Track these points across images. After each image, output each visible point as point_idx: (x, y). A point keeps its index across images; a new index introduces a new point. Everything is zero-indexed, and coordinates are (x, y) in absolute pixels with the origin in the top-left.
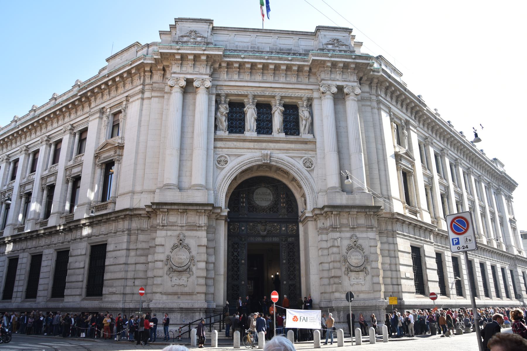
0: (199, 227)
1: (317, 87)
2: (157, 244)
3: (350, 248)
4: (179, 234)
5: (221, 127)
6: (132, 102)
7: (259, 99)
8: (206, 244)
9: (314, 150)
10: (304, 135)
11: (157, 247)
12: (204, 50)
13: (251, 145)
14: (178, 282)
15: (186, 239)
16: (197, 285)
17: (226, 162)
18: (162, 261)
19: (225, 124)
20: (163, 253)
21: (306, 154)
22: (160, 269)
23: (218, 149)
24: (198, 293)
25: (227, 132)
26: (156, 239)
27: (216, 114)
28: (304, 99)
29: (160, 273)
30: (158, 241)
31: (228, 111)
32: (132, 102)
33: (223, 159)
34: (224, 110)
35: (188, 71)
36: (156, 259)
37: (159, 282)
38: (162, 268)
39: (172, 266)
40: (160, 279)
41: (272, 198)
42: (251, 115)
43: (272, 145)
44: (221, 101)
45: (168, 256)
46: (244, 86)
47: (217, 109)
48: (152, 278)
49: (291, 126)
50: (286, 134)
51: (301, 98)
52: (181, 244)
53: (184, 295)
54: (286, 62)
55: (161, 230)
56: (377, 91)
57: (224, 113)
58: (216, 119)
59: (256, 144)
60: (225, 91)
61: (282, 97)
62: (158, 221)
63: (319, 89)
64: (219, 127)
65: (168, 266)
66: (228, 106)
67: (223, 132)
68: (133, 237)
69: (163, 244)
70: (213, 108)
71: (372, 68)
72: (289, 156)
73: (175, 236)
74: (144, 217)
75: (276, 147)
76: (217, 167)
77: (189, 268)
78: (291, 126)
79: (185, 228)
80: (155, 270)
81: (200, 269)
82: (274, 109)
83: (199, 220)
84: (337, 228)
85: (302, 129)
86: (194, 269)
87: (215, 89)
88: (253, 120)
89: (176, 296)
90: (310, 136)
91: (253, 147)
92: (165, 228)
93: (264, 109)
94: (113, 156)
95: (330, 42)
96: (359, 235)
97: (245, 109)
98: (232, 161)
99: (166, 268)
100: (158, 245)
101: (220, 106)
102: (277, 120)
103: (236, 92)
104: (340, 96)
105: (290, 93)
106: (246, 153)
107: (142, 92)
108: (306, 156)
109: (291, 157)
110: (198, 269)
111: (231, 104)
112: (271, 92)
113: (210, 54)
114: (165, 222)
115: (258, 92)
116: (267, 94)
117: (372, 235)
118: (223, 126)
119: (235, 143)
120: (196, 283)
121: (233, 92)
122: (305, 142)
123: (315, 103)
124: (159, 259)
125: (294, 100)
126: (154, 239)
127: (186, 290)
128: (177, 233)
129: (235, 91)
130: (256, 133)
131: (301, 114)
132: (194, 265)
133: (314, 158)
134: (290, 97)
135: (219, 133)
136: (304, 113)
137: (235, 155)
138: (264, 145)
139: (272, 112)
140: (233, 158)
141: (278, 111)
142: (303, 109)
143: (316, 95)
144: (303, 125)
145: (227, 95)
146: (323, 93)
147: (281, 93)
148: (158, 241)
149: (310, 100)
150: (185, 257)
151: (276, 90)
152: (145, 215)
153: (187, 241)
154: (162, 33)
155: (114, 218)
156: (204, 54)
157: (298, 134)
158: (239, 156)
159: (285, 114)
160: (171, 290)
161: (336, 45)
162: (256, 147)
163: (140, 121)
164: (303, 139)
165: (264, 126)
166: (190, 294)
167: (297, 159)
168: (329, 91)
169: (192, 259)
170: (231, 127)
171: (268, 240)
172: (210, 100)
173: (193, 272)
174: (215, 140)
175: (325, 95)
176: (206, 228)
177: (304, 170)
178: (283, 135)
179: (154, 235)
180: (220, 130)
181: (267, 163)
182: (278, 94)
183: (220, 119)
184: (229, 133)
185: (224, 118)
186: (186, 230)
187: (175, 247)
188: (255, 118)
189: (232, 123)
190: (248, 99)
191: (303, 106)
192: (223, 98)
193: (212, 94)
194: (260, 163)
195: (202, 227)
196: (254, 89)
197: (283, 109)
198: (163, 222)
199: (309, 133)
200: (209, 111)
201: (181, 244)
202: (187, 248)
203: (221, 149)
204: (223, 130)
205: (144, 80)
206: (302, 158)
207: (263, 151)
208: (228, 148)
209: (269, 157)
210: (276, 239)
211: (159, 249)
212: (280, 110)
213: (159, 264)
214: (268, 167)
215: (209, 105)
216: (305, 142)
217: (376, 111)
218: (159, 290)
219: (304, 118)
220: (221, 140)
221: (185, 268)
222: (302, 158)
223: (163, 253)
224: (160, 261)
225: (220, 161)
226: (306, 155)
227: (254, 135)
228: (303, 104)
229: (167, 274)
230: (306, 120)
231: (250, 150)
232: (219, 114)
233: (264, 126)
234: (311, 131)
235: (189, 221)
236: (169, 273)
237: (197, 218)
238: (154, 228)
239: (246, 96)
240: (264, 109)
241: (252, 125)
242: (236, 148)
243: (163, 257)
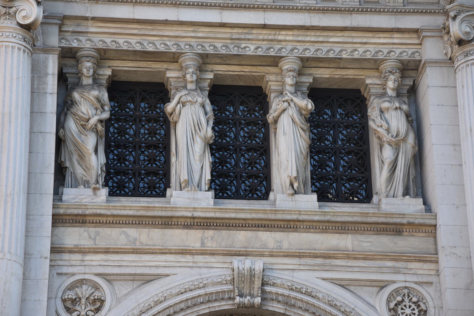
1: (439, 20)
5: (79, 171)
7: (222, 69)
9: (431, 257)
10: (390, 201)
13: (193, 238)
19: (96, 162)
21: (397, 271)
23: (66, 256)
25: (104, 192)
27: (60, 124)
28: (388, 66)
31: (106, 115)
33: (85, 291)
34: (91, 111)
42: (191, 127)
43: (269, 239)
44: (79, 75)
46: (166, 23)
47: (65, 106)
49: (341, 167)
50: (322, 198)
51: (375, 64)
57: (93, 121)
58: (60, 142)
59: (210, 233)
60: (96, 39)
61: (306, 63)
63: (446, 29)
64: (73, 174)
66: (105, 96)
67: (89, 191)
70: (51, 104)
72: (332, 281)
75: (285, 246)
78: (341, 167)
82: (276, 105)
85: (380, 178)
87: (56, 29)
88: (199, 146)
90: (412, 206)
91: (197, 245)
93: (239, 108)
97: (169, 107)
98: (119, 301)
101: (76, 95)
102: (288, 147)
103: (134, 43)
105: (333, 46)
108: (400, 280)
109: (344, 285)
111: (119, 89)
112: (265, 45)
115: (219, 44)
116: (251, 49)
118: (87, 169)
119: (133, 232)
121: (122, 43)
122: (395, 228)
123: (431, 85)
125: (350, 73)
129: (133, 40)
130: (211, 194)
131: (375, 122)
133: (431, 290)
134: (336, 62)
135: (69, 194)
136: (386, 119)
137: (134, 277)
138: (241, 238)
139: (270, 118)
140: (122, 288)
141: (292, 111)
142: (386, 105)
143: (432, 50)
144: (384, 164)
145: (103, 56)
146: (460, 42)
147: (301, 47)
149: (410, 71)
157: (368, 199)
158: (147, 279)
159: (314, 123)
162: (211, 245)
164: (387, 215)
165: (240, 169)
167: (364, 292)
170: (117, 173)
172: (36, 72)
174: (58, 220)
175: (467, 48)
178: (309, 201)
180: (75, 184)
181: (252, 306)
182: (292, 48)
183: (76, 145)
184: (111, 194)
185: (90, 141)
188: (205, 139)
189: (122, 159)
190: (181, 69)
191: (383, 95)
192: (87, 67)
193: (47, 50)
194: (225, 306)
196: (203, 32)
197: (309, 105)
199: (406, 193)
200: (35, 113)
203: (78, 257)
204: (86, 184)
206: (382, 286)
207: (237, 262)
208: (107, 251)
209: (258, 283)
212: (300, 110)
215: (36, 92)
216: (395, 228)
219: (386, 137)
220: (80, 220)
222: (382, 286)
225: (74, 301)
226: (400, 277)
227: (206, 199)
228: (384, 86)
230: (397, 147)
231: (189, 258)
232: (72, 125)
233: (240, 169)
234: (416, 184)
239: (174, 58)
240: (239, 108)
241: (196, 167)
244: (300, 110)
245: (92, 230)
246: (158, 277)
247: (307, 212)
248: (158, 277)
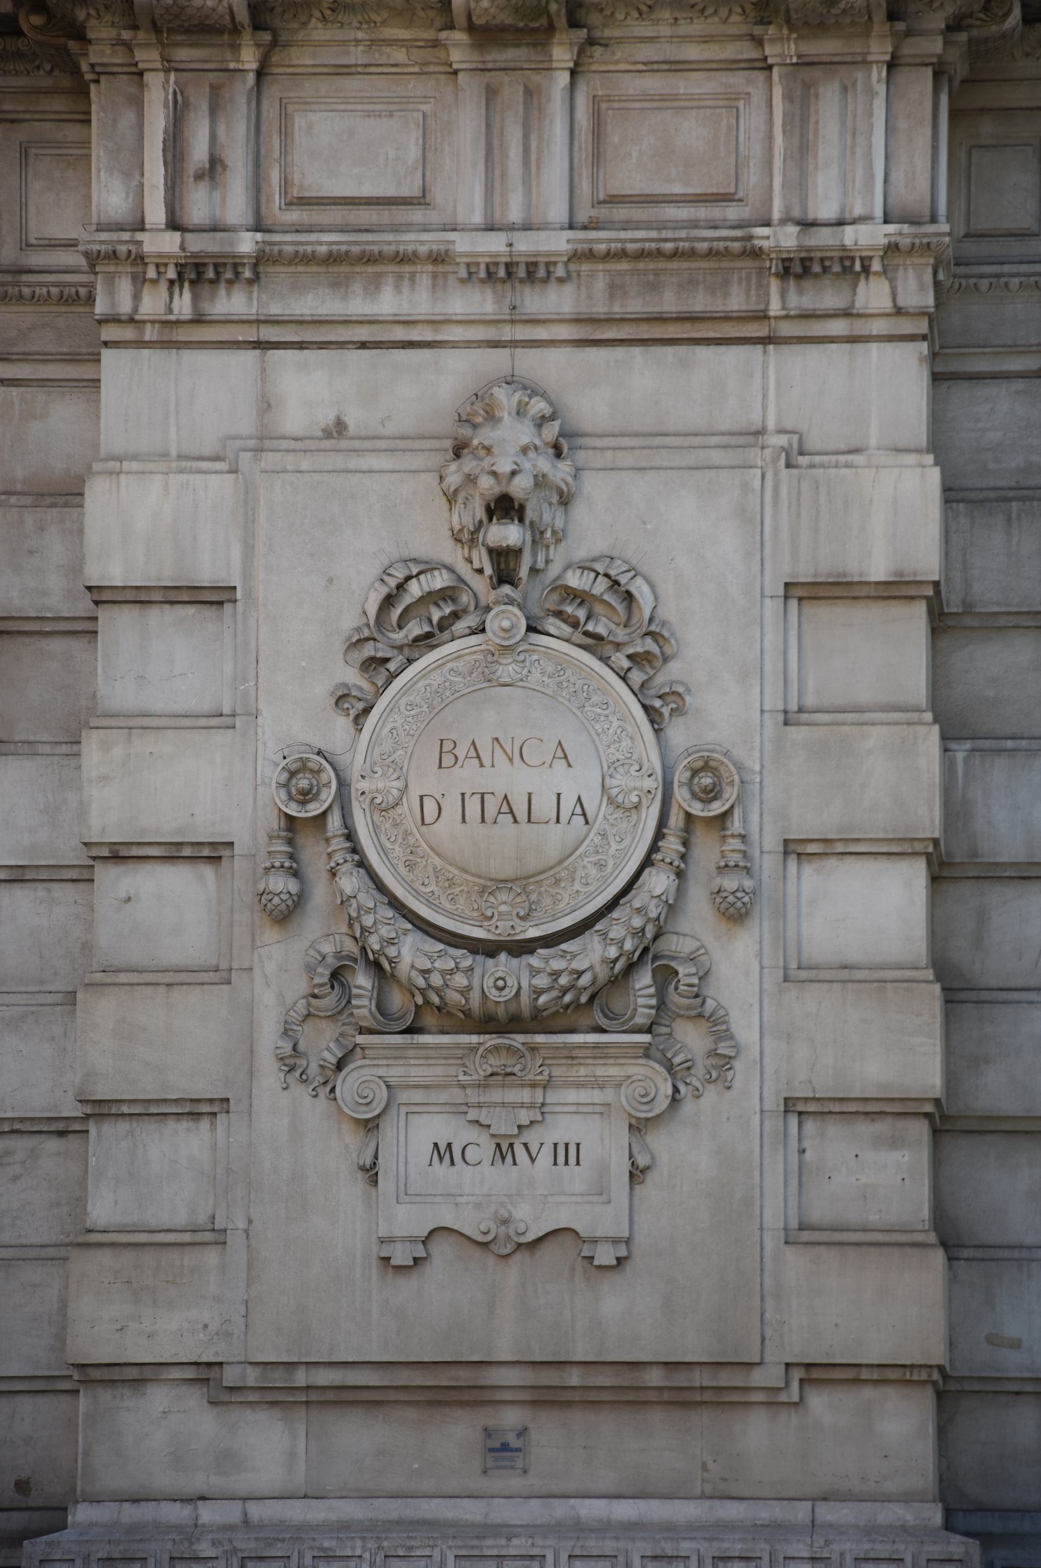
0: (798, 268)
2: (114, 573)
4: (478, 410)
8: (926, 560)
11: (119, 626)
14: (478, 1191)
15: (597, 491)
16: (804, 1233)
18: (213, 854)
20: (220, 720)
24: (815, 1373)
26: (98, 495)
29: (180, 1043)
30: (130, 527)
36: (108, 816)
37: (175, 1206)
38: (219, 975)
39: (383, 925)
40: (191, 1142)
45: (301, 775)
48: (62, 1129)
53: (590, 1400)
55: (171, 336)
62: (111, 198)
65: (319, 936)
73: (404, 441)
77: (647, 954)
79: (557, 300)
80: (103, 1011)
81: (844, 974)
83: (802, 150)
86: (736, 969)
89: (456, 1436)
92: (232, 303)
100: (139, 598)
110: (798, 973)
114: (236, 206)
120: (774, 1213)
124: (163, 822)
126: (65, 494)
127: (623, 1320)
132: (735, 913)
148: (130, 527)
150: (580, 782)
160: (368, 1326)
166: (694, 1390)
173: (716, 1024)
176: (916, 290)
179: (54, 429)
186: (594, 333)
195: (850, 267)
198: (199, 206)
201: (504, 566)
202: (616, 626)
211: (151, 663)
221: (592, 955)
223: (220, 720)
224: (174, 853)
229: (291, 1063)
235: (628, 175)
236: (322, 1043)
237: (763, 113)
243: (219, 789)
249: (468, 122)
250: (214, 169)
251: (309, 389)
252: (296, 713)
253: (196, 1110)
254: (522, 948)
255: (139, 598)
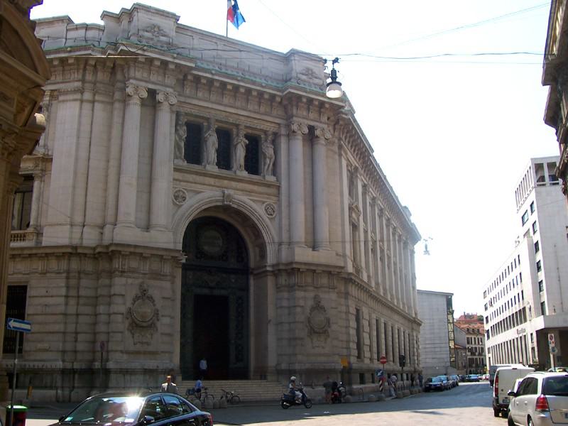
0: (163, 276)
3: (313, 309)
4: (143, 283)
6: (63, 101)
7: (220, 124)
12: (174, 58)
13: (212, 181)
17: (184, 199)
18: (123, 314)
21: (268, 198)
22: (120, 324)
24: (162, 352)
32: (63, 101)
35: (156, 80)
41: (220, 242)
46: (208, 108)
49: (253, 164)
51: (265, 132)
52: (143, 295)
54: (258, 88)
56: (340, 134)
60: (186, 109)
68: (73, 282)
69: (123, 293)
71: (343, 111)
72: (251, 200)
74: (89, 257)
76: (174, 204)
78: (253, 164)
84: (302, 287)
94: (32, 170)
95: (304, 72)
96: (322, 295)
98: (190, 198)
99: (127, 323)
104: (311, 137)
105: (256, 124)
106: (206, 193)
107: (81, 91)
108: (269, 201)
109: (254, 201)
113: (180, 64)
114: (126, 267)
115: (221, 116)
116: (231, 120)
117: (333, 296)
119: (194, 176)
122: (269, 186)
127: (151, 348)
128: (140, 280)
136: (268, 150)
143: (283, 131)
148: (116, 289)
149: (276, 135)
151: (241, 118)
152: (92, 256)
153: (150, 292)
154: (105, 15)
155: (43, 255)
156: (173, 63)
158: (198, 193)
159: (248, 148)
160: (132, 348)
161: (310, 76)
162: (217, 184)
163: (79, 130)
164: (267, 181)
165: (225, 160)
168: (300, 130)
169: (156, 313)
171: (217, 292)
177: (265, 217)
178: (245, 174)
186: (149, 279)
187: (136, 298)
194: (219, 204)
195: (166, 276)
196: (218, 112)
202: (151, 298)
205: (84, 76)
210: (223, 292)
211: (118, 300)
212: (245, 143)
213: (119, 318)
214: (227, 209)
216: (269, 186)
217: (337, 157)
218: (119, 349)
221: (150, 323)
224: (120, 314)
233: (225, 160)
234: (274, 173)
238: (111, 274)
240: (225, 138)
242: (195, 183)
243: (123, 309)
244: (245, 143)
245: (182, 174)
246: (202, 192)
247: (244, 177)
248: (202, 192)
249: (142, 263)
250: (125, 265)
251: (130, 281)
252: (129, 304)
253: (121, 332)
254: (145, 322)
255: (119, 295)
